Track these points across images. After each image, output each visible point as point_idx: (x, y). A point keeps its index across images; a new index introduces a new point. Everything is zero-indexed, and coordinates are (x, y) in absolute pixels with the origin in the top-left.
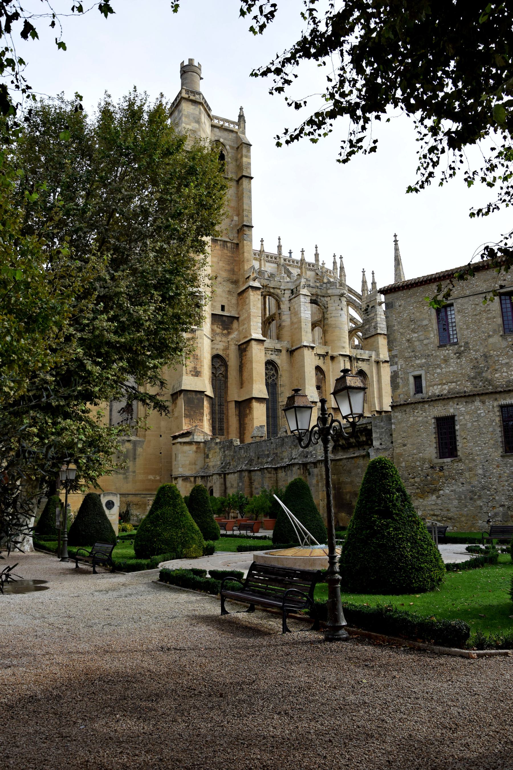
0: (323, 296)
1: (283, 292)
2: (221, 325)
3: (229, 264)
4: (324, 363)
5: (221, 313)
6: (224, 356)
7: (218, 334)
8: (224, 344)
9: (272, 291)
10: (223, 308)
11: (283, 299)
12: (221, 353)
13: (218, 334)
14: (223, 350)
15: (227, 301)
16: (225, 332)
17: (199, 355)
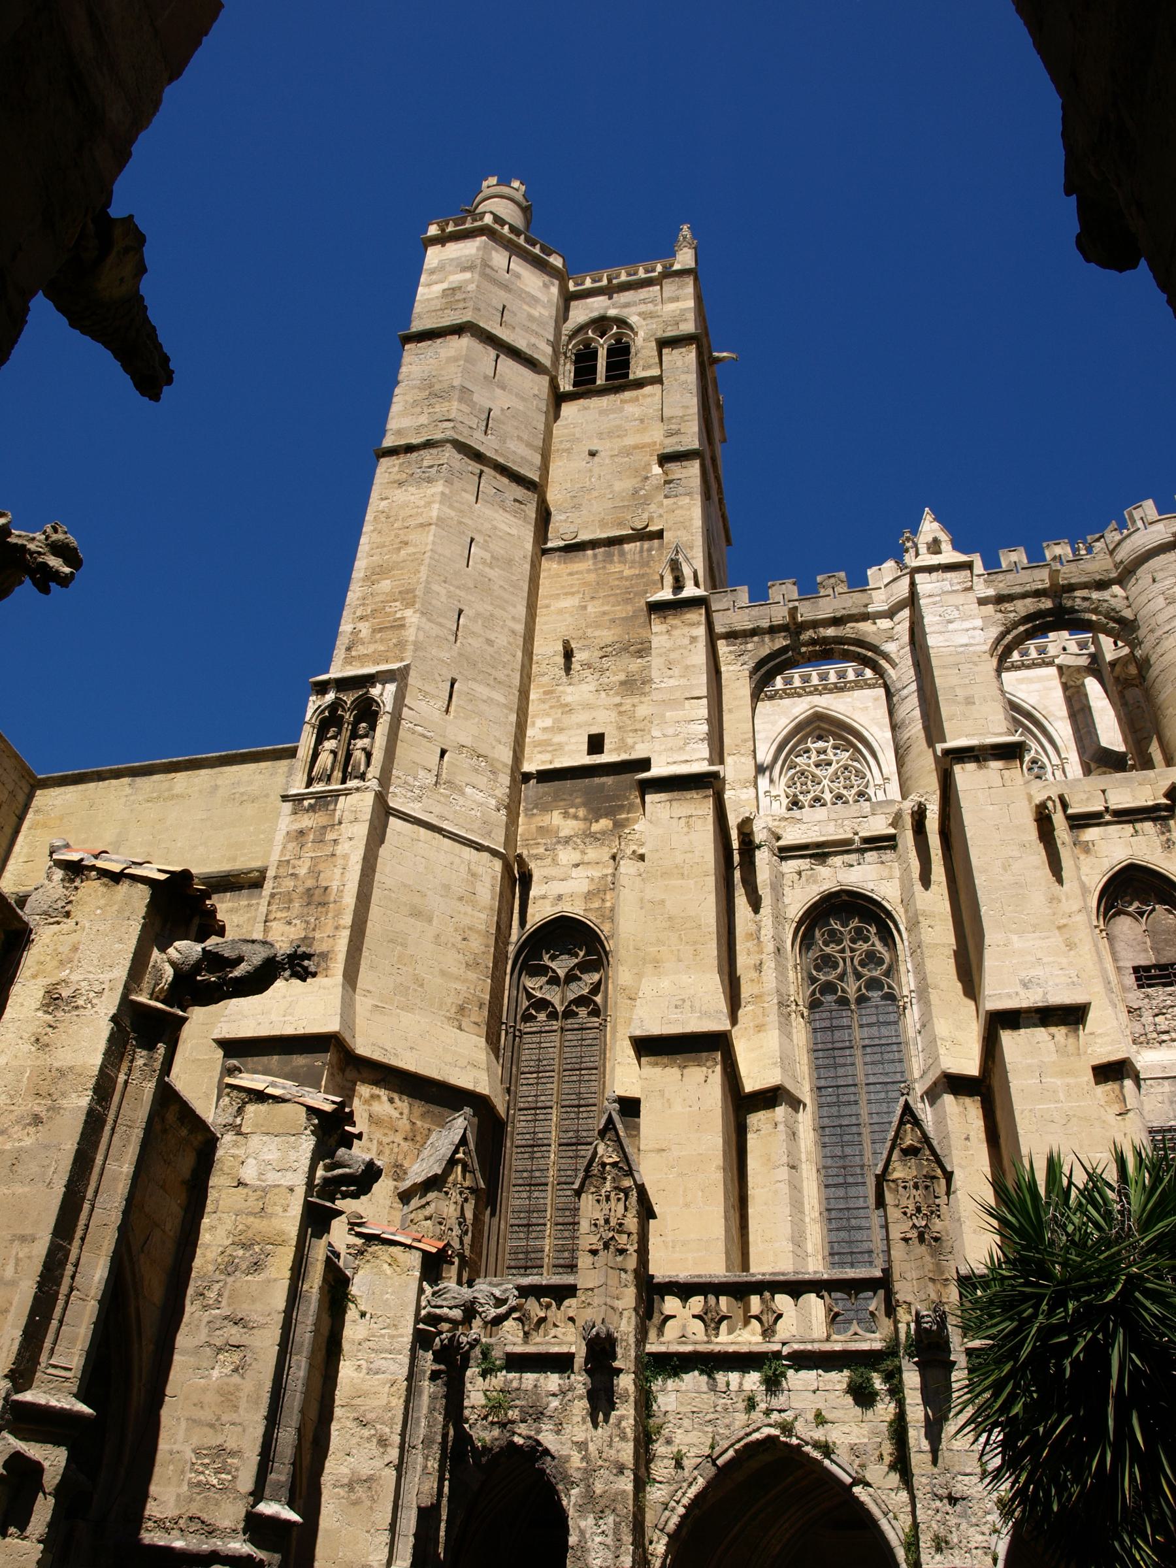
0: (1102, 585)
1: (884, 624)
2: (584, 804)
3: (627, 601)
4: (1168, 845)
5: (585, 759)
6: (592, 919)
7: (567, 841)
8: (596, 873)
9: (830, 632)
10: (596, 743)
11: (890, 648)
12: (575, 909)
13: (567, 841)
14: (589, 896)
15: (613, 715)
16: (604, 823)
17: (334, 885)
